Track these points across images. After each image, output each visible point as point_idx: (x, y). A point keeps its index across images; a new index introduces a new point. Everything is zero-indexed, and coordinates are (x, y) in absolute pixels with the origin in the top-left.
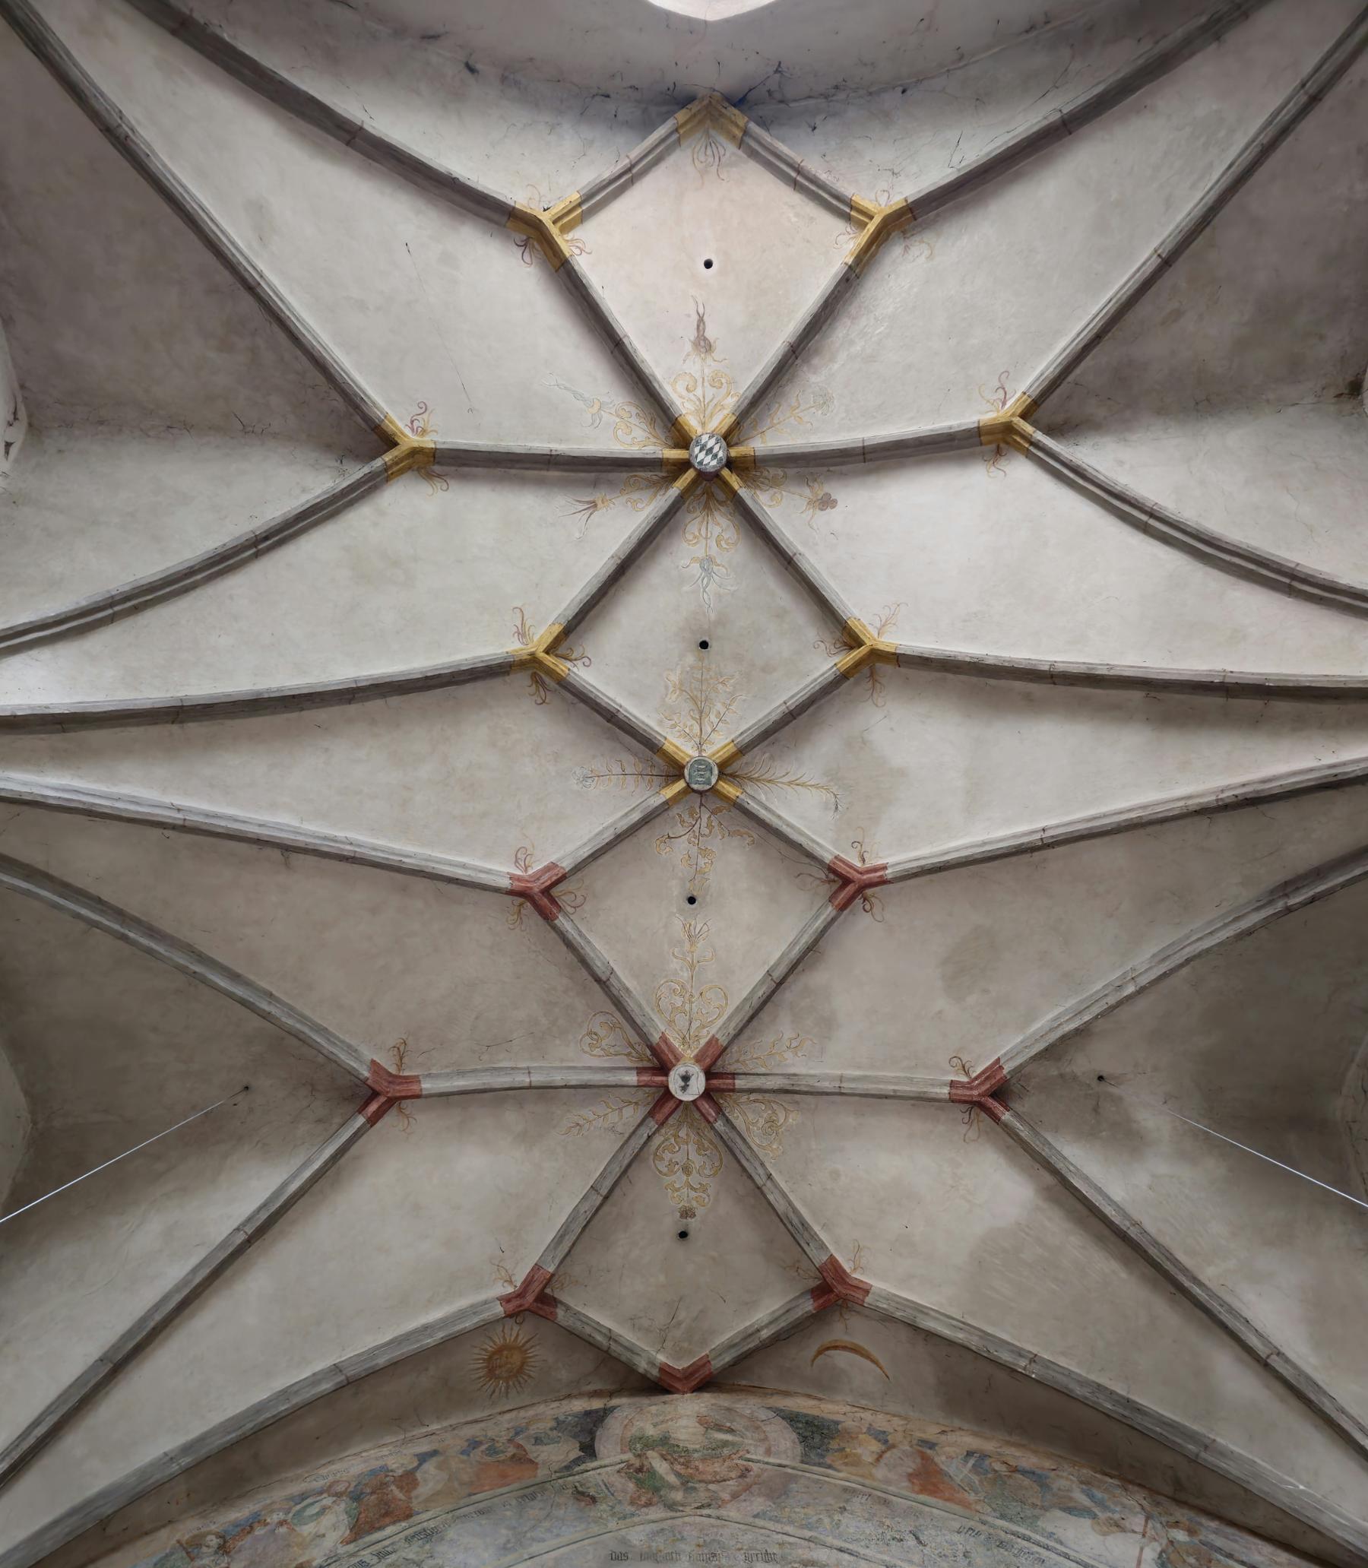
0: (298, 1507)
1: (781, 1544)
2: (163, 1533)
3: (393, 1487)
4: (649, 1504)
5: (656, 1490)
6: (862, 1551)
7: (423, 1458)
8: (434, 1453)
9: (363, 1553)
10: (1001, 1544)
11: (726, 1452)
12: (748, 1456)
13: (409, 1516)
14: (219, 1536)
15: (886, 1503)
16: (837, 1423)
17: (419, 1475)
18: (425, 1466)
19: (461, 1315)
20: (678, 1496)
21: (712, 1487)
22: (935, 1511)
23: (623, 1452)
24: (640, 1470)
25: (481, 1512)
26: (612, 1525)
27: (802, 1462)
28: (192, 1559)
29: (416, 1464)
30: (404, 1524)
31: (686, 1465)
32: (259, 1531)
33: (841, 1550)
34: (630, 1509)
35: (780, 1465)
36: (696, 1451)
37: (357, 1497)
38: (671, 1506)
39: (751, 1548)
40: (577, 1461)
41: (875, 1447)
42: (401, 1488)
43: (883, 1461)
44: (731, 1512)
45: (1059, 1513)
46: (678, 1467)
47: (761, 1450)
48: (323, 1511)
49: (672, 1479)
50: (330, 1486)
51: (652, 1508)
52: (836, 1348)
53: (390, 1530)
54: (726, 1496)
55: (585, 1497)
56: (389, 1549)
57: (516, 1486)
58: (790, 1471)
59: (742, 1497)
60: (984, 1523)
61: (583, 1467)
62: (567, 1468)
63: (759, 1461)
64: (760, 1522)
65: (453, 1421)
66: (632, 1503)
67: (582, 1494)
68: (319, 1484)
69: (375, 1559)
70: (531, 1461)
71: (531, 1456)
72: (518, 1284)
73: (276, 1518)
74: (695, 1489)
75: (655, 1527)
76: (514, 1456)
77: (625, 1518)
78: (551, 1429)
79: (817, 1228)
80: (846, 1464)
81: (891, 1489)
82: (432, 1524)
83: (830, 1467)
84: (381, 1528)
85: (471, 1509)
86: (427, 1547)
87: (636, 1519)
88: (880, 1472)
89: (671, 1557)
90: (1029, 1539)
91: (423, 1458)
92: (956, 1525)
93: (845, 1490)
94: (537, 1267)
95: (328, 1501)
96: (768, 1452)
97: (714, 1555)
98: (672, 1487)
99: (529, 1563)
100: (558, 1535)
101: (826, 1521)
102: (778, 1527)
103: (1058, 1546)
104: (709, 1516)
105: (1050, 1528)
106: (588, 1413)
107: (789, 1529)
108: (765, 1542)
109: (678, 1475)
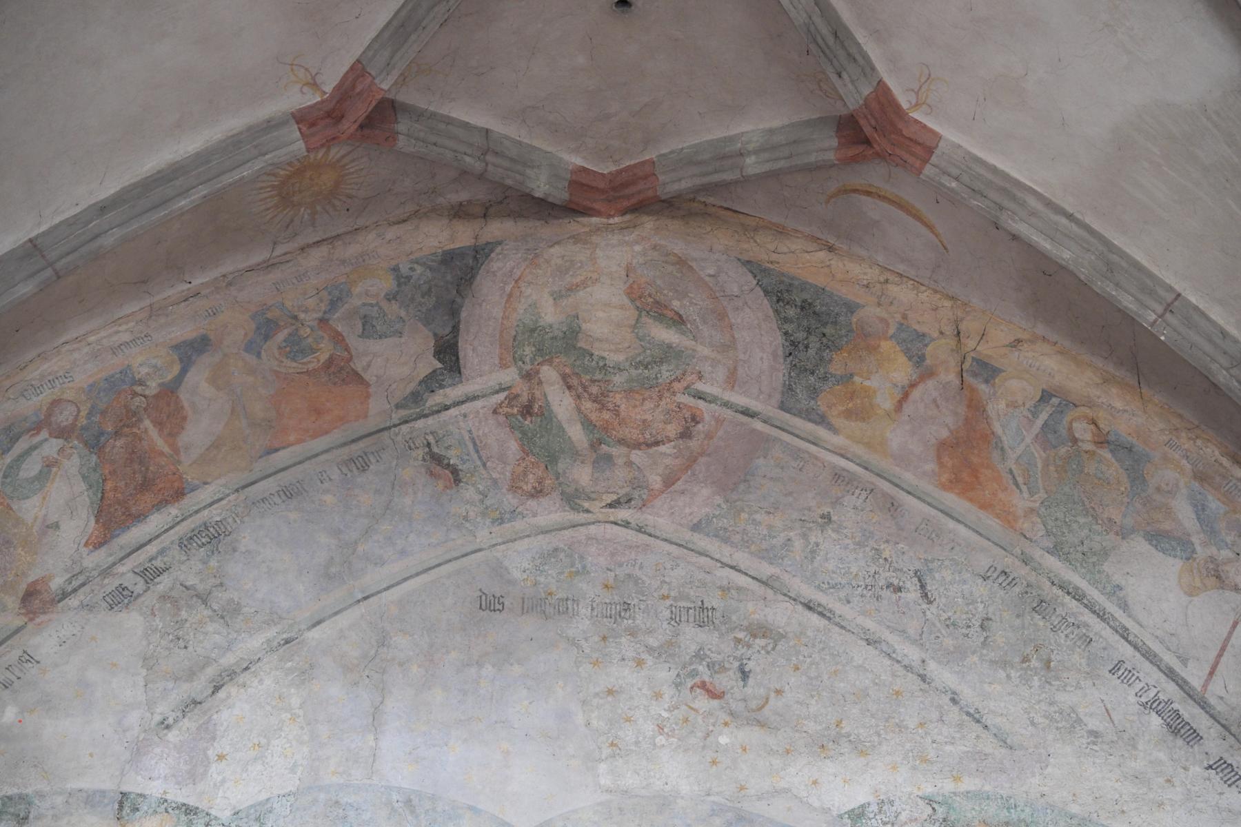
1: (725, 590)
3: (147, 423)
4: (537, 493)
5: (552, 459)
6: (839, 608)
8: (201, 345)
9: (121, 569)
10: (1041, 606)
11: (666, 373)
12: (700, 386)
13: (179, 494)
15: (893, 507)
16: (851, 308)
17: (184, 396)
18: (193, 377)
19: (234, 143)
20: (582, 475)
21: (637, 456)
22: (962, 530)
23: (503, 366)
24: (527, 411)
25: (288, 493)
26: (483, 535)
27: (783, 407)
29: (176, 369)
33: (809, 607)
34: (510, 500)
35: (747, 412)
36: (619, 369)
37: (95, 444)
38: (572, 499)
40: (431, 383)
41: (902, 371)
42: (159, 424)
43: (908, 408)
44: (659, 518)
45: (1140, 545)
46: (588, 405)
47: (721, 373)
48: (50, 465)
49: (576, 433)
50: (49, 415)
51: (544, 501)
52: (869, 193)
53: (155, 522)
54: (655, 481)
55: (444, 469)
56: (158, 563)
57: (336, 436)
59: (679, 485)
60: (1026, 560)
61: (437, 398)
62: (416, 397)
63: (713, 400)
64: (701, 542)
65: (228, 267)
66: (514, 488)
67: (438, 459)
68: (31, 405)
69: (141, 586)
70: (357, 378)
71: (358, 365)
72: (328, 88)
74: (609, 458)
76: (330, 361)
77: (501, 521)
78: (391, 297)
79: (860, 36)
80: (848, 414)
81: (908, 477)
82: (214, 514)
83: (822, 420)
84: (140, 517)
85: (269, 485)
86: (213, 563)
87: (519, 525)
88: (897, 436)
89: (563, 608)
90: (1078, 596)
92: (983, 562)
93: (838, 476)
94: (358, 71)
95: (52, 447)
96: (732, 380)
97: (627, 607)
98: (575, 454)
100: (403, 553)
101: (798, 544)
103: (1119, 614)
104: (626, 525)
105: (1117, 579)
106: (448, 258)
107: (741, 558)
108: (704, 585)
109: (588, 424)
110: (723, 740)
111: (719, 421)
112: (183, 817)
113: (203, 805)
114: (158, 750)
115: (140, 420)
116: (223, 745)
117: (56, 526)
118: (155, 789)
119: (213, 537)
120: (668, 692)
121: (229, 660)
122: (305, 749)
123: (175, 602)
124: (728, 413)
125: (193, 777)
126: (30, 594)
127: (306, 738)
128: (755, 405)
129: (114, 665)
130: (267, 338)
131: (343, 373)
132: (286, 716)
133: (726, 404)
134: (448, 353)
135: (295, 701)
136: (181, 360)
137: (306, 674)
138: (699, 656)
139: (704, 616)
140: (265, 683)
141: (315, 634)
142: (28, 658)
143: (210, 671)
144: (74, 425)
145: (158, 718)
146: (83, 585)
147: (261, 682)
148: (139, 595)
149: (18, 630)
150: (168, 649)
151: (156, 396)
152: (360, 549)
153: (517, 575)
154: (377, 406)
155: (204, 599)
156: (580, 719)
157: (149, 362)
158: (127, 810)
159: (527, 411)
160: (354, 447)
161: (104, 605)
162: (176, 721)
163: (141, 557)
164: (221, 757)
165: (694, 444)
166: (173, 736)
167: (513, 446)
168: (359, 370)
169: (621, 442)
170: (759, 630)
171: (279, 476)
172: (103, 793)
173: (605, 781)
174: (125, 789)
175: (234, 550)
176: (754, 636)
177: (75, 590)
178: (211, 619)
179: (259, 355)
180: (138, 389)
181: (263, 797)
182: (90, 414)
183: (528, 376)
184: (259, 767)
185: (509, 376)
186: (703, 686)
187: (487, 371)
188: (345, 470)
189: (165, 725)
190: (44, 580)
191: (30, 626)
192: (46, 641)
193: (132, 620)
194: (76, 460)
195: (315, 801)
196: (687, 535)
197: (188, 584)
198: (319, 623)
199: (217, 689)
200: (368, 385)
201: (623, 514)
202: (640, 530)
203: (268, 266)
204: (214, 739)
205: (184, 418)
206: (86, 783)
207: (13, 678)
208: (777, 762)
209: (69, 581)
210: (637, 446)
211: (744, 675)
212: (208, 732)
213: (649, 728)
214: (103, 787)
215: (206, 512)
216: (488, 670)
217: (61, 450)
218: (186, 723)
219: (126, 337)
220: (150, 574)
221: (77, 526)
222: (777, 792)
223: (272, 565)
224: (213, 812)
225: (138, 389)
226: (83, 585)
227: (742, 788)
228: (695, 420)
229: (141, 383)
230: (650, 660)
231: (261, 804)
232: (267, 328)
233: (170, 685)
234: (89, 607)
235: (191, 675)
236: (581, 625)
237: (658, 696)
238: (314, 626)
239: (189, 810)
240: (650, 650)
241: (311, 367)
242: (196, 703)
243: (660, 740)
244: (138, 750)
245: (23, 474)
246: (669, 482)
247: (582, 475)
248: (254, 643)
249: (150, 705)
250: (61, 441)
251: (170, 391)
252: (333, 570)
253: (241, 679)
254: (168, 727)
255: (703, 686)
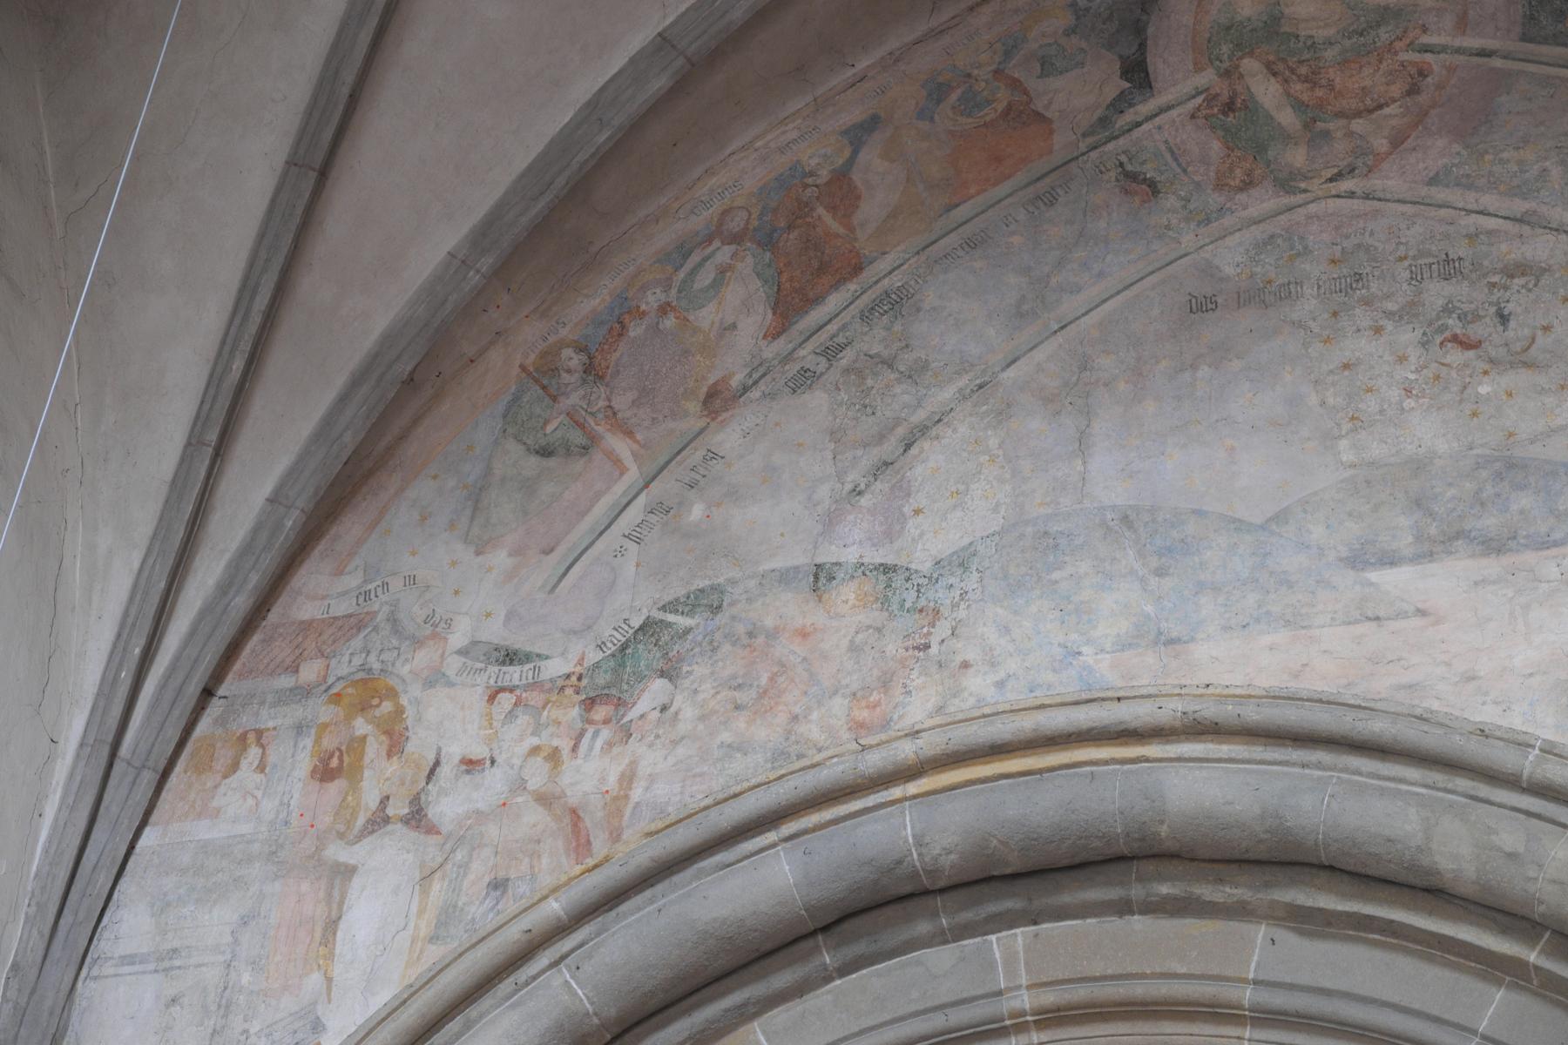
0: (681, 275)
1: (1472, 237)
2: (495, 356)
3: (821, 210)
4: (1247, 185)
5: (1260, 149)
7: (858, 135)
8: (872, 123)
9: (802, 353)
11: (1384, 34)
12: (1426, 39)
13: (858, 269)
14: (581, 349)
17: (856, 177)
18: (863, 156)
20: (1297, 157)
21: (1358, 125)
23: (1198, 68)
24: (1229, 107)
25: (971, 244)
26: (1188, 240)
27: (1525, 38)
28: (554, 399)
29: (847, 153)
30: (852, 286)
31: (1311, 81)
32: (636, 330)
34: (1215, 199)
35: (1483, 53)
36: (1330, 43)
37: (768, 241)
38: (1287, 183)
39: (1422, 254)
40: (1120, 104)
42: (832, 209)
44: (1389, 181)
46: (1297, 87)
48: (723, 271)
49: (1287, 118)
50: (721, 223)
51: (1254, 192)
53: (834, 301)
54: (1381, 144)
55: (1139, 185)
56: (840, 339)
57: (1021, 178)
58: (1497, 63)
59: (1410, 143)
62: (1104, 122)
63: (1443, 49)
64: (1440, 194)
65: (893, 44)
66: (1220, 186)
67: (1133, 177)
68: (699, 221)
70: (1039, 117)
71: (1039, 105)
73: (652, 300)
74: (1326, 134)
75: (1257, 233)
77: (1208, 221)
78: (1069, 32)
82: (896, 280)
84: (818, 300)
85: (953, 239)
86: (897, 327)
87: (1227, 221)
89: (1287, 293)
91: (858, 135)
95: (724, 254)
96: (1462, 24)
97: (1359, 277)
98: (1287, 138)
99: (1060, 338)
100: (1101, 275)
102: (1470, 199)
104: (1352, 195)
107: (1489, 201)
108: (1447, 236)
109: (1299, 106)
110: (1484, 390)
111: (1451, 69)
112: (882, 577)
113: (902, 562)
114: (851, 517)
115: (812, 209)
116: (919, 500)
117: (734, 326)
118: (850, 555)
119: (895, 303)
120: (1414, 355)
121: (920, 416)
122: (1008, 487)
123: (860, 374)
124: (1461, 59)
125: (890, 536)
126: (712, 395)
127: (1008, 476)
128: (1491, 44)
129: (800, 445)
130: (939, 102)
131: (1025, 116)
132: (984, 458)
133: (1459, 51)
134: (1137, 74)
135: (993, 442)
136: (851, 143)
137: (1003, 413)
138: (1447, 310)
139: (1449, 268)
140: (961, 430)
141: (1011, 373)
142: (713, 455)
143: (901, 431)
144: (746, 228)
145: (849, 487)
146: (764, 375)
147: (955, 430)
148: (822, 374)
149: (700, 433)
150: (856, 419)
151: (828, 183)
152: (1054, 281)
153: (1229, 270)
154: (1059, 140)
155: (889, 364)
156: (1313, 400)
157: (818, 154)
158: (822, 580)
159: (1229, 107)
160: (1039, 185)
161: (787, 390)
162: (867, 486)
163: (823, 336)
164: (917, 512)
165: (1423, 98)
166: (864, 501)
167: (1216, 145)
168: (1040, 110)
169: (1340, 115)
170: (1519, 269)
171: (960, 230)
172: (796, 569)
173: (1348, 457)
174: (819, 561)
175: (918, 310)
176: (1512, 277)
177: (756, 383)
178: (899, 381)
179: (932, 120)
180: (810, 181)
181: (966, 541)
182: (762, 214)
183: (1227, 74)
184: (959, 513)
185: (1207, 78)
186: (1455, 339)
187: (1180, 79)
188: (1031, 209)
189: (857, 492)
190: (725, 380)
191: (713, 425)
192: (729, 437)
193: (817, 400)
194: (750, 260)
195: (1022, 536)
196: (1424, 191)
197: (872, 353)
198: (1014, 362)
199: (908, 447)
200: (1049, 121)
201: (1346, 185)
202: (1367, 197)
203: (938, 33)
204: (909, 495)
205: (859, 198)
206: (778, 563)
207: (698, 477)
208: (1550, 400)
209: (750, 375)
210: (1358, 114)
211: (1503, 318)
212: (903, 490)
213: (1395, 394)
214: (796, 563)
215: (886, 281)
216: (1204, 371)
217: (734, 255)
218: (878, 485)
219: (794, 135)
220: (831, 352)
221: (754, 323)
222: (1553, 432)
223: (960, 319)
224: (913, 566)
225: (810, 181)
226: (764, 375)
227: (1511, 435)
228: (1422, 74)
229: (812, 174)
230: (1389, 326)
231: (964, 549)
232: (938, 91)
233: (859, 452)
234: (771, 396)
235: (881, 438)
236: (1308, 305)
237: (1402, 359)
238: (1009, 365)
239: (886, 569)
240: (1389, 315)
241: (988, 119)
242: (887, 464)
243: (1409, 403)
244: (830, 521)
245: (697, 286)
246: (1397, 141)
247: (1297, 157)
248: (948, 393)
249: (840, 476)
250: (733, 247)
251: (841, 177)
252: (1025, 307)
253: (934, 432)
254: (860, 493)
255: (1455, 339)
